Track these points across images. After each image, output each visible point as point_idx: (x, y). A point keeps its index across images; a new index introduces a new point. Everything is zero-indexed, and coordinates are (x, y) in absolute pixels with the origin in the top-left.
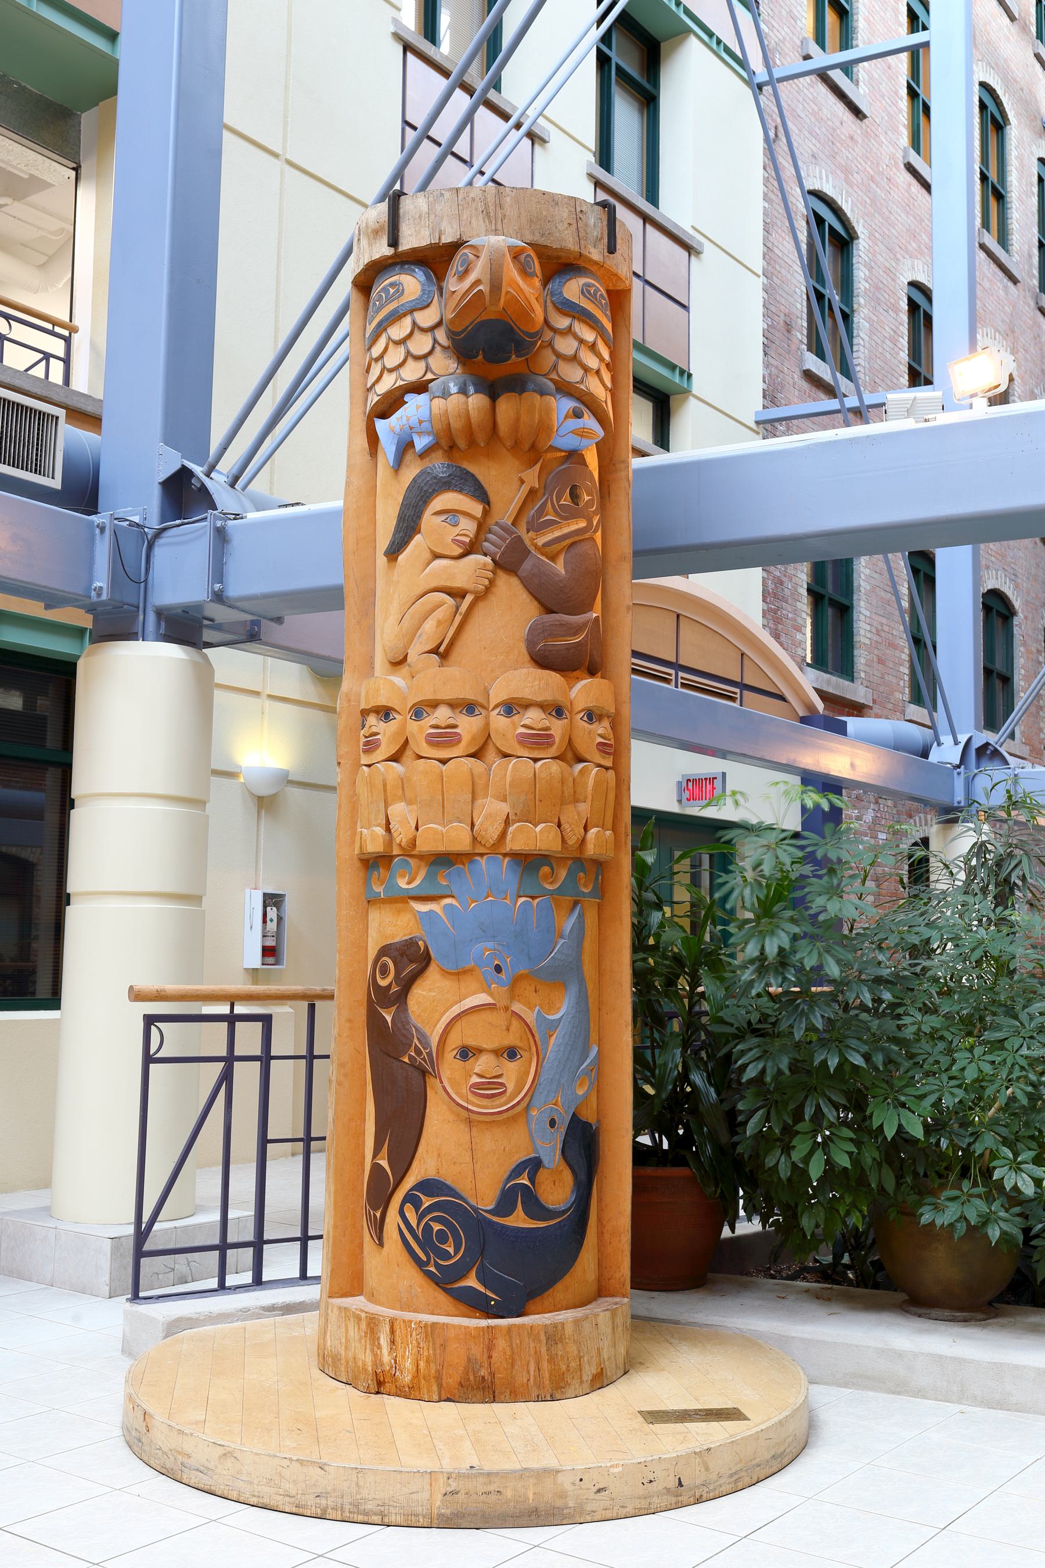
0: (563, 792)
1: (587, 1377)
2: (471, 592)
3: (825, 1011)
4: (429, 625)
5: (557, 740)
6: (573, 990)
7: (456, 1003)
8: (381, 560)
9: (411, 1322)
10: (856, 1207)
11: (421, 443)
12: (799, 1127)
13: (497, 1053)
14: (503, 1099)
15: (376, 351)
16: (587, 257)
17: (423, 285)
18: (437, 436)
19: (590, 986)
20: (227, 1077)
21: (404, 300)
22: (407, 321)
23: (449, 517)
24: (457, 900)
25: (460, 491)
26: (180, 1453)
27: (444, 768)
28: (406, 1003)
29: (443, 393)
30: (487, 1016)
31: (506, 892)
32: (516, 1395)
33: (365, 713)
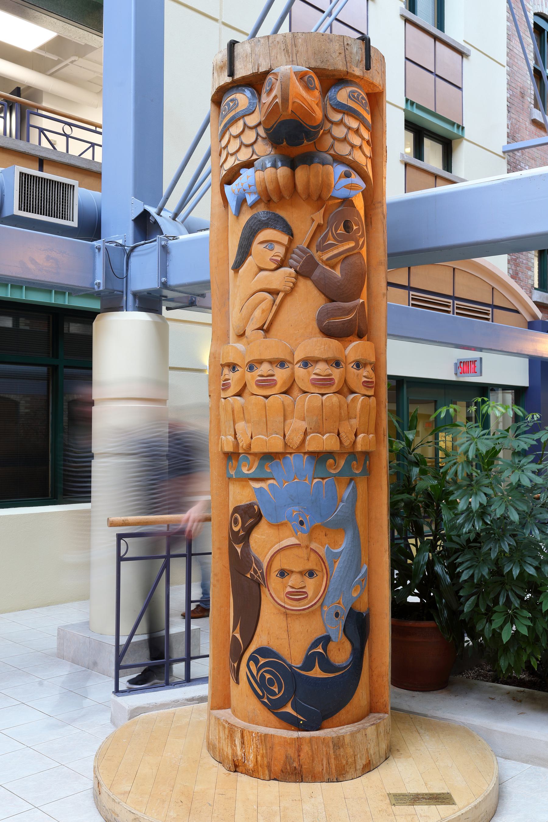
0: (340, 413)
1: (360, 766)
2: (282, 291)
3: (510, 541)
4: (257, 313)
5: (336, 381)
6: (350, 534)
7: (277, 543)
8: (231, 272)
9: (253, 732)
10: (534, 656)
11: (250, 199)
12: (495, 609)
13: (301, 573)
14: (306, 601)
15: (224, 143)
16: (351, 74)
17: (250, 99)
18: (259, 195)
19: (361, 529)
20: (167, 566)
21: (239, 109)
22: (241, 123)
23: (269, 245)
24: (277, 481)
25: (275, 228)
26: (113, 812)
27: (267, 401)
28: (248, 542)
29: (262, 168)
30: (296, 551)
31: (305, 476)
32: (315, 778)
33: (223, 366)
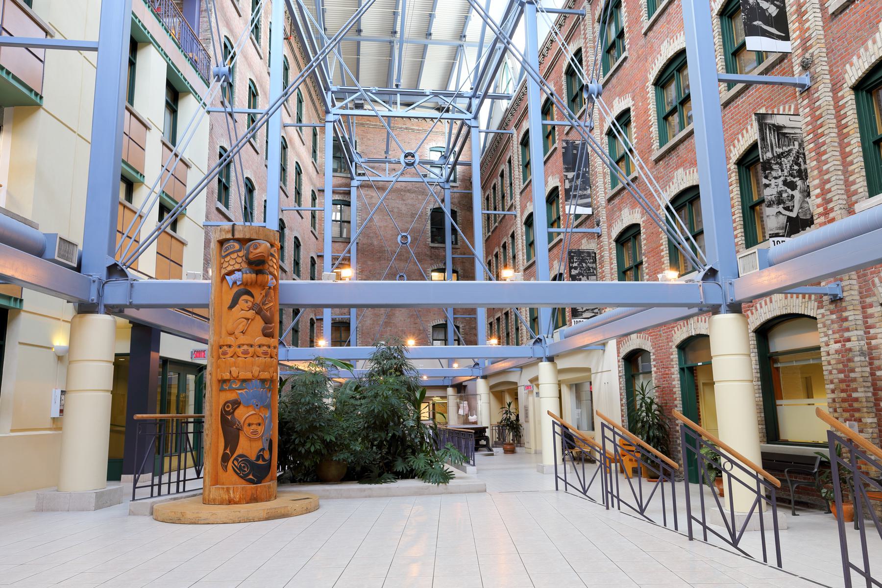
11: (238, 283)
